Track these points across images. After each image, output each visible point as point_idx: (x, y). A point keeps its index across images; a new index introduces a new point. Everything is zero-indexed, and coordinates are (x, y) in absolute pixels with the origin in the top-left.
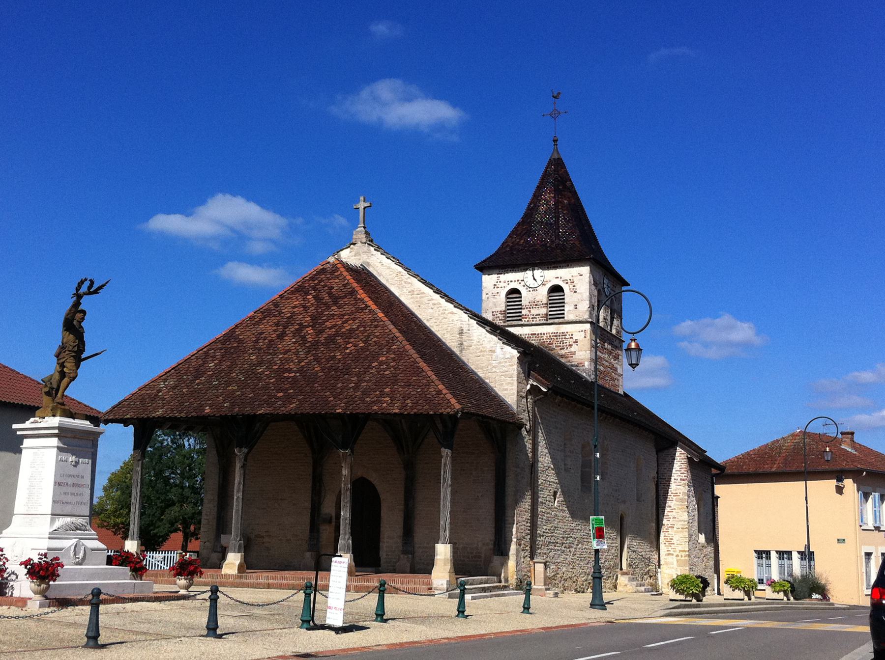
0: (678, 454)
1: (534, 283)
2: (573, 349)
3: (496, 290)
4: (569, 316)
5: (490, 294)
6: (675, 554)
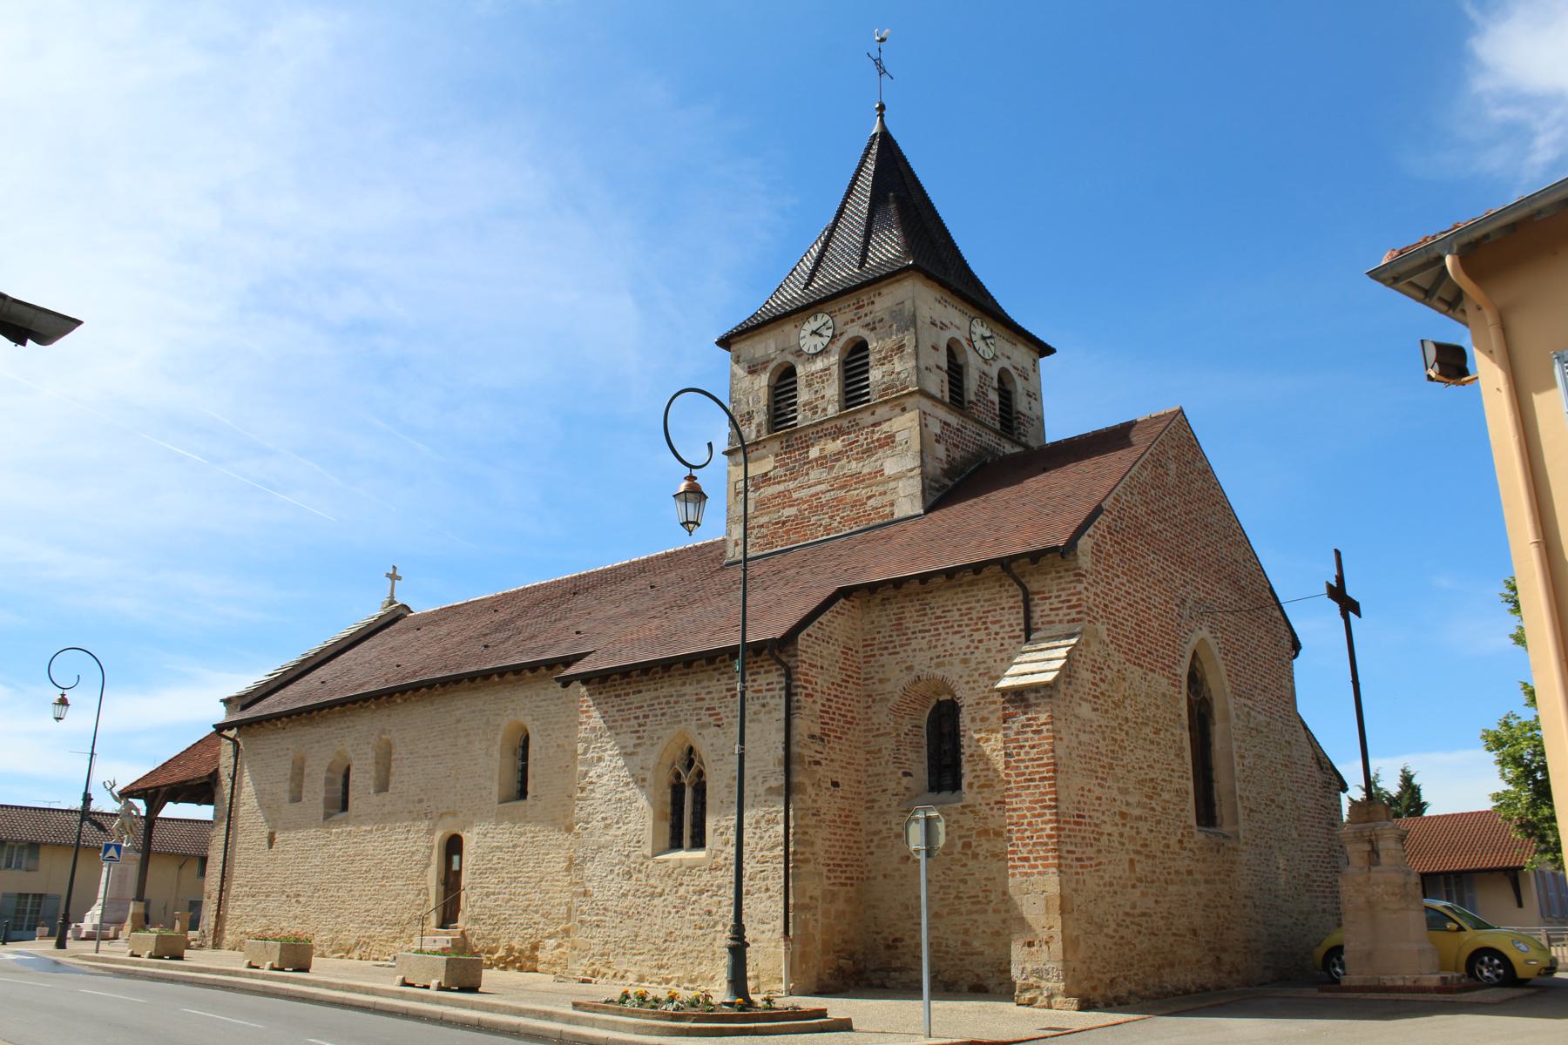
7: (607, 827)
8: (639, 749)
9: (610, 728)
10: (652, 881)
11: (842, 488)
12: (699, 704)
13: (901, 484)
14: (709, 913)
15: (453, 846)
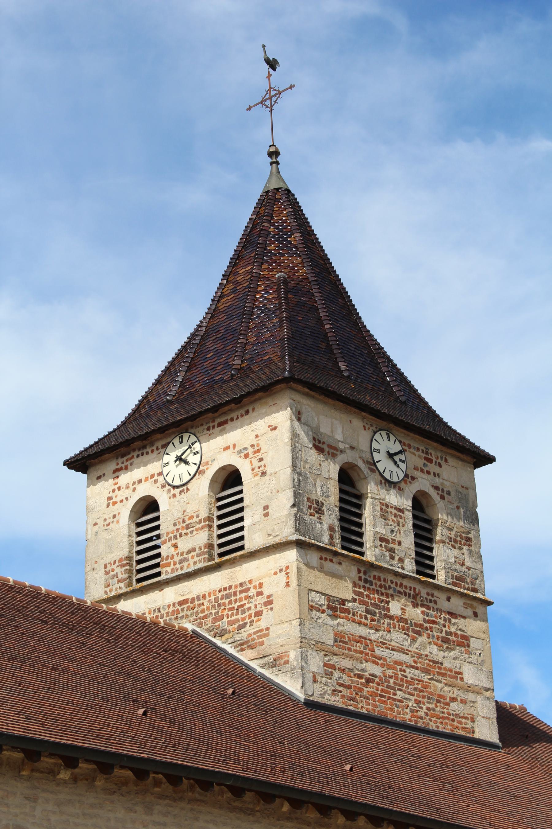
2: (262, 624)
3: (114, 509)
4: (253, 540)
5: (101, 522)
11: (426, 671)
13: (479, 699)
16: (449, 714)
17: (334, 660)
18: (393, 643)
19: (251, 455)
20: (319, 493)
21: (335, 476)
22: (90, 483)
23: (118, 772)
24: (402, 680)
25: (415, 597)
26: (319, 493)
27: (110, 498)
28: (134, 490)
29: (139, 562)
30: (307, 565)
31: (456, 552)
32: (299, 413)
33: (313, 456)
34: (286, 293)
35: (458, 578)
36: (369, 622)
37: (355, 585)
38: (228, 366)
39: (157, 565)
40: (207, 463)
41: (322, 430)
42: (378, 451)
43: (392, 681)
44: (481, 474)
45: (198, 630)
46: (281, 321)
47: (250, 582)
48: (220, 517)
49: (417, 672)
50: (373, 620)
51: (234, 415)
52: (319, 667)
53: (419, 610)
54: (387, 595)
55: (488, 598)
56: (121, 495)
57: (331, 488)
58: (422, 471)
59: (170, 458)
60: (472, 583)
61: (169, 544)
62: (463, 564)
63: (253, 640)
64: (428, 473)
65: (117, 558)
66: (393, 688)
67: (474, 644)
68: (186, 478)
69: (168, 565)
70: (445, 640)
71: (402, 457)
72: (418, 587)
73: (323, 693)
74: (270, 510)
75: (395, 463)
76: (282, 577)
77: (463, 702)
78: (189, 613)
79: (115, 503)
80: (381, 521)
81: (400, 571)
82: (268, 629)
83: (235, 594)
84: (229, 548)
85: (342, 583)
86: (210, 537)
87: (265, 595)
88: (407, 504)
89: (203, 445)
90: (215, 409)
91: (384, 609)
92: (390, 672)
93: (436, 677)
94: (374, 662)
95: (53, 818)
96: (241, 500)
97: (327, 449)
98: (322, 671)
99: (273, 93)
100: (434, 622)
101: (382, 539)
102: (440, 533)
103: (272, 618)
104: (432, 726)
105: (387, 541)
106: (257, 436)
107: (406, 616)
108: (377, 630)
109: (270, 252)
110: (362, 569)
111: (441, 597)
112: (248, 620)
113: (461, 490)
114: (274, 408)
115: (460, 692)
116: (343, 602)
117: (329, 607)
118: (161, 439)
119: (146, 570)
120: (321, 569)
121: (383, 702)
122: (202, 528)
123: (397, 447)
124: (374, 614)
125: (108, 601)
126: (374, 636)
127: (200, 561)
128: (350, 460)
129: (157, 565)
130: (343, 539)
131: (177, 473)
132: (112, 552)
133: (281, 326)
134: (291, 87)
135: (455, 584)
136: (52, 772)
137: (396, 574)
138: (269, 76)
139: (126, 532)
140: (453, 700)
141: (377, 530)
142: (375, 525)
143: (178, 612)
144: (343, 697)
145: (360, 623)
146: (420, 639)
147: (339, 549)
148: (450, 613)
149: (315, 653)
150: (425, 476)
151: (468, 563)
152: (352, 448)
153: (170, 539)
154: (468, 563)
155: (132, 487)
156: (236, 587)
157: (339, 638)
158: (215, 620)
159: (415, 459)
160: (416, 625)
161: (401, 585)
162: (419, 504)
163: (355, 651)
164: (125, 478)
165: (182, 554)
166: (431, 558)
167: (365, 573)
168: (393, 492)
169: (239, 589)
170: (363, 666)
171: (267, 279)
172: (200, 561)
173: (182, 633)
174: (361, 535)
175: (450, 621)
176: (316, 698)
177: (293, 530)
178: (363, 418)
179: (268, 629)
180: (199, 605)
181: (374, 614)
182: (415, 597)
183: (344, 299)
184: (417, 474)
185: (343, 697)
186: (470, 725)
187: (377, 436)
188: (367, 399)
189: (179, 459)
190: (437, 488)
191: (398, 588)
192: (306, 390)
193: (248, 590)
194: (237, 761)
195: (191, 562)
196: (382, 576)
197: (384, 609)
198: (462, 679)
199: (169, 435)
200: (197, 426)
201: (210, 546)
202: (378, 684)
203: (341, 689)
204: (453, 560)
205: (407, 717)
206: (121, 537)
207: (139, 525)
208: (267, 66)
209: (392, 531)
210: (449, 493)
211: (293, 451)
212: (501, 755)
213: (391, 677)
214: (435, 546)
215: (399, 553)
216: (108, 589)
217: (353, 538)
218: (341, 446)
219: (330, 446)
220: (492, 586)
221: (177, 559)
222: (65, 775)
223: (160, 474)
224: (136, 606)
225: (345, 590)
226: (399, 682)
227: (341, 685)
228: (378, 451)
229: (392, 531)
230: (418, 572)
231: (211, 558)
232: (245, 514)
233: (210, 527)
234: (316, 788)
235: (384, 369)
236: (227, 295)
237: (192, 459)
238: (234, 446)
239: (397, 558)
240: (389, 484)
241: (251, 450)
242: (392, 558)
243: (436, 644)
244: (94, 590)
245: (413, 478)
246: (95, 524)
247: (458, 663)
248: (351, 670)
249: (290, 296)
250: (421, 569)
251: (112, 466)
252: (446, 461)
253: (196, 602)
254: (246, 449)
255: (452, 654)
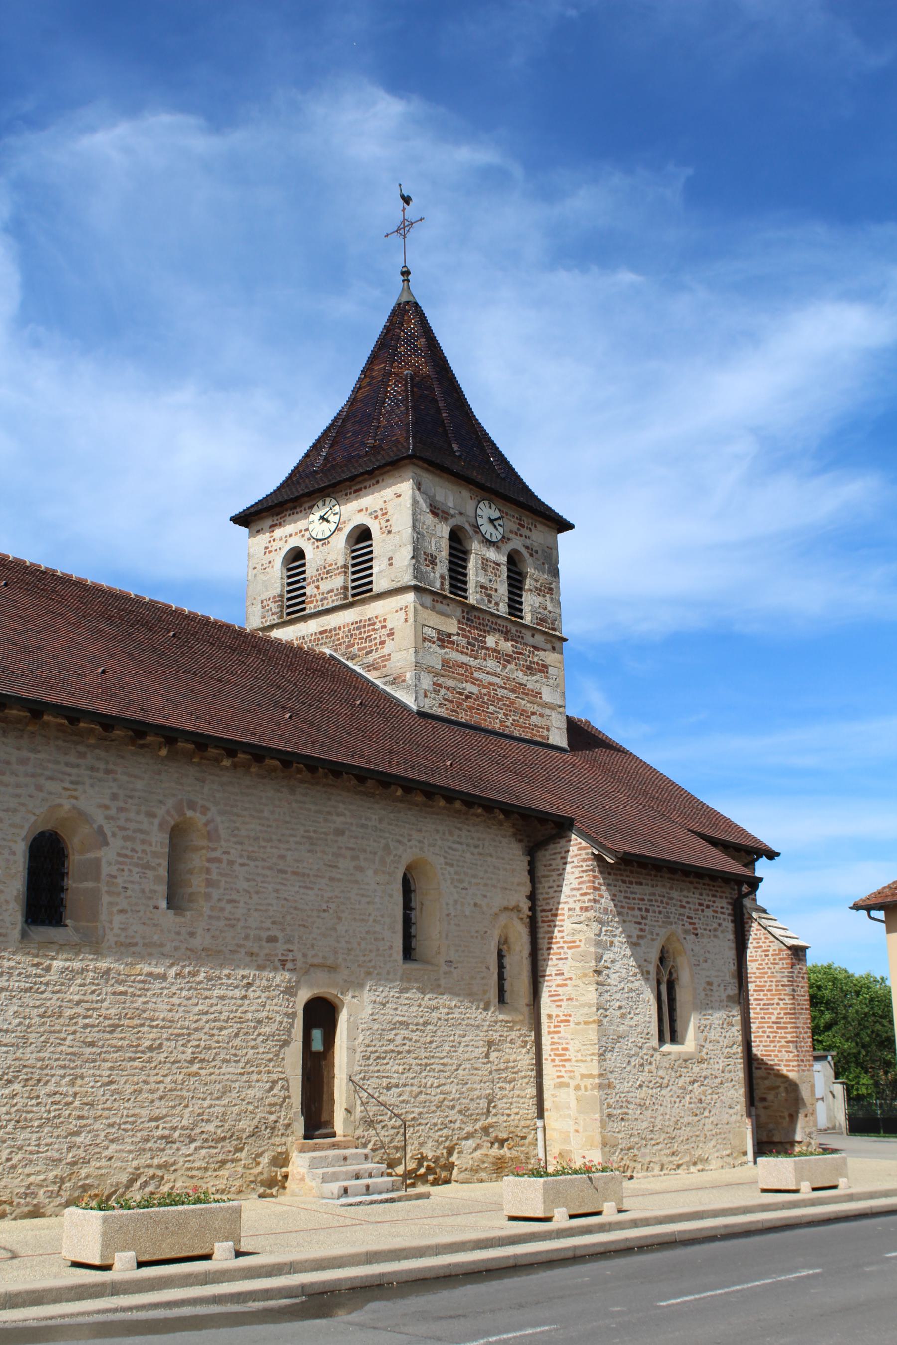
0: (573, 850)
1: (322, 530)
2: (386, 651)
4: (380, 584)
5: (259, 567)
6: (573, 1084)
7: (623, 1016)
8: (641, 942)
9: (619, 913)
10: (661, 1073)
11: (513, 691)
12: (682, 910)
14: (700, 1101)
15: (321, 1015)
16: (530, 724)
17: (441, 680)
18: (488, 669)
19: (380, 517)
20: (433, 549)
21: (447, 535)
22: (251, 535)
23: (268, 761)
24: (494, 697)
25: (506, 633)
26: (433, 549)
27: (266, 548)
28: (286, 542)
29: (289, 599)
30: (422, 605)
31: (541, 599)
32: (419, 484)
33: (429, 519)
34: (412, 387)
35: (541, 619)
36: (469, 652)
37: (459, 622)
38: (364, 445)
39: (303, 602)
40: (345, 522)
41: (437, 498)
42: (482, 517)
43: (486, 698)
44: (563, 538)
45: (334, 654)
46: (407, 409)
47: (377, 617)
48: (354, 566)
49: (506, 692)
50: (472, 650)
51: (367, 484)
52: (429, 685)
53: (509, 644)
54: (485, 631)
55: (564, 635)
56: (275, 545)
57: (443, 545)
58: (516, 534)
59: (315, 516)
60: (552, 624)
61: (313, 586)
62: (545, 609)
63: (378, 663)
64: (521, 535)
65: (271, 596)
66: (487, 704)
67: (551, 670)
68: (328, 534)
69: (312, 602)
70: (529, 668)
71: (501, 522)
72: (510, 626)
73: (431, 706)
74: (393, 561)
75: (495, 526)
76: (402, 614)
77: (541, 715)
78: (327, 641)
79: (270, 552)
80: (481, 572)
81: (496, 612)
82: (389, 655)
83: (364, 626)
84: (360, 590)
85: (449, 621)
86: (346, 581)
87: (388, 628)
88: (503, 559)
89: (342, 507)
90: (352, 479)
91: (482, 641)
92: (484, 691)
93: (521, 696)
94: (472, 683)
95: (218, 795)
96: (371, 552)
97: (441, 514)
98: (431, 689)
99: (407, 223)
100: (521, 653)
101: (482, 587)
102: (528, 584)
103: (392, 645)
104: (516, 734)
105: (486, 588)
106: (385, 502)
107: (499, 648)
108: (476, 658)
109: (400, 353)
110: (466, 610)
111: (527, 634)
112: (374, 648)
113: (546, 549)
114: (399, 479)
115: (538, 708)
116: (450, 635)
117: (438, 639)
118: (309, 501)
119: (294, 606)
120: (433, 609)
121: (478, 714)
122: (340, 573)
123: (497, 514)
124: (474, 645)
125: (264, 629)
126: (473, 662)
127: (337, 600)
128: (459, 523)
129: (303, 602)
130: (452, 585)
131: (320, 529)
132: (267, 591)
133: (407, 414)
134: (421, 220)
135: (538, 624)
136: (217, 760)
137: (492, 614)
138: (404, 209)
139: (279, 575)
140: (533, 714)
141: (479, 579)
142: (477, 576)
143: (319, 639)
144: (447, 709)
145: (462, 652)
146: (509, 666)
147: (449, 595)
148: (534, 647)
149: (426, 675)
150: (518, 538)
151: (550, 608)
152: (461, 513)
153: (314, 582)
154: (550, 608)
155: (284, 540)
156: (365, 621)
157: (446, 663)
158: (348, 647)
159: (511, 524)
160: (507, 655)
161: (496, 623)
162: (513, 560)
163: (458, 674)
164: (279, 532)
165: (323, 594)
166: (521, 603)
167: (468, 613)
168: (492, 549)
169: (367, 623)
170: (464, 686)
171: (397, 375)
172: (337, 600)
173: (321, 656)
174: (465, 583)
175: (533, 653)
176: (426, 710)
177: (412, 578)
178: (471, 490)
179: (389, 655)
180: (336, 635)
181: (474, 645)
182: (506, 633)
183: (458, 393)
184: (512, 536)
185: (447, 709)
186: (545, 733)
187: (481, 505)
188: (474, 475)
189: (322, 518)
190: (527, 548)
191: (494, 626)
192: (425, 466)
193: (375, 623)
194: (362, 756)
195: (330, 600)
196: (481, 616)
197: (482, 641)
198: (541, 698)
199: (315, 499)
200: (338, 492)
201: (345, 588)
202: (475, 700)
203: (446, 703)
204: (537, 605)
205: (497, 726)
206: (275, 579)
207: (289, 570)
208: (402, 201)
209: (491, 581)
210: (536, 552)
211: (413, 514)
212: (568, 757)
213: (485, 695)
214: (524, 594)
215: (496, 597)
216: (264, 620)
217: (459, 585)
218: (452, 511)
219: (443, 512)
220: (567, 628)
221: (319, 598)
222: (227, 762)
223: (307, 529)
224: (286, 634)
225: (451, 626)
226: (491, 699)
227: (446, 700)
228: (482, 517)
229: (491, 581)
230: (510, 614)
231: (346, 598)
232: (374, 563)
233: (346, 573)
234: (423, 778)
235: (489, 451)
236: (365, 387)
237: (333, 518)
238: (367, 509)
239: (493, 602)
240: (489, 543)
241: (379, 513)
242: (490, 602)
243: (522, 670)
244: (253, 621)
245: (509, 539)
246: (255, 568)
247: (538, 685)
248: (454, 689)
249: (415, 389)
250: (513, 611)
251: (269, 522)
252: (535, 526)
253: (334, 632)
254: (376, 511)
255: (534, 678)
